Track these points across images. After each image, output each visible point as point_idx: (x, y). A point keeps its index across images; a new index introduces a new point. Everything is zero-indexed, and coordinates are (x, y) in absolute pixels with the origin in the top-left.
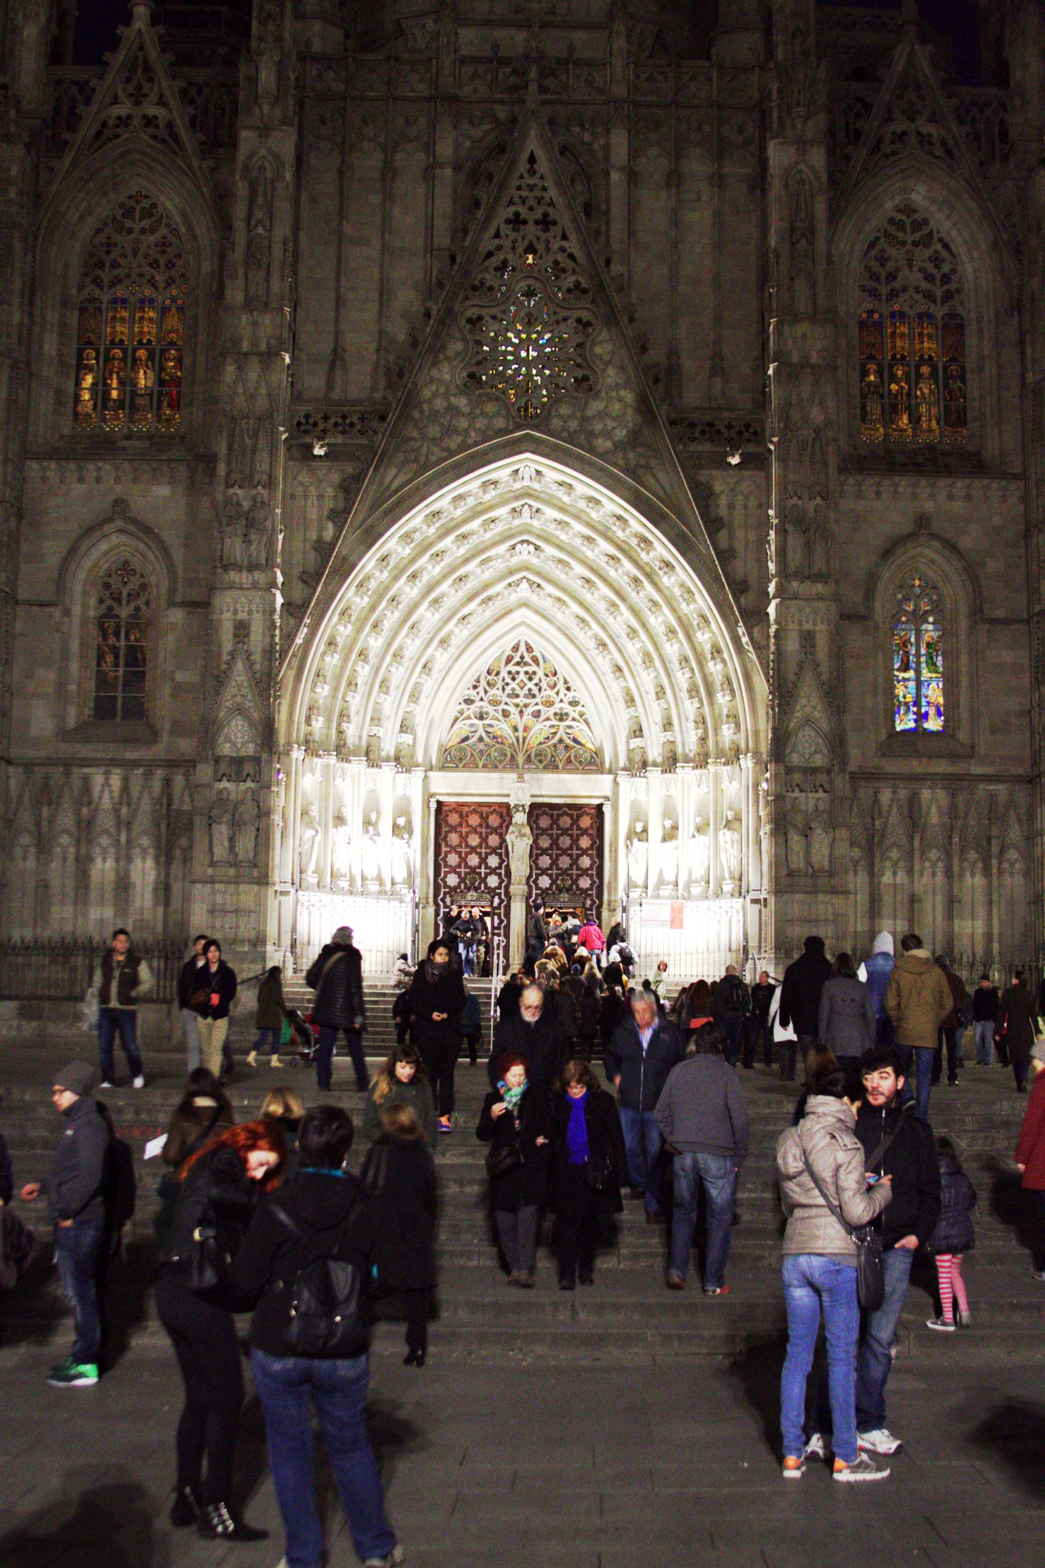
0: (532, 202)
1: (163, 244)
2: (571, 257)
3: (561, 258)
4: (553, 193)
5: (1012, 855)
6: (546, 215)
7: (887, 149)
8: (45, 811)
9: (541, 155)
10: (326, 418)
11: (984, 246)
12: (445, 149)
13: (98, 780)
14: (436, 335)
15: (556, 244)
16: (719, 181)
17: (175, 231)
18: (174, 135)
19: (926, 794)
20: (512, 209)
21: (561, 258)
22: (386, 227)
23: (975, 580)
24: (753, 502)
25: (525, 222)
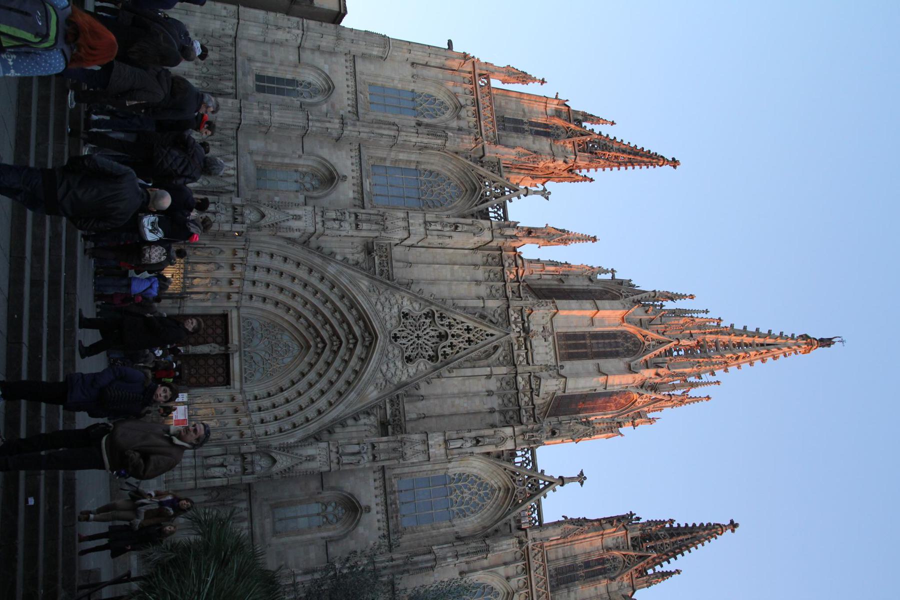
2: (458, 352)
4: (481, 343)
8: (218, 143)
12: (492, 304)
13: (232, 165)
14: (421, 298)
15: (461, 345)
16: (492, 411)
19: (245, 524)
24: (367, 433)
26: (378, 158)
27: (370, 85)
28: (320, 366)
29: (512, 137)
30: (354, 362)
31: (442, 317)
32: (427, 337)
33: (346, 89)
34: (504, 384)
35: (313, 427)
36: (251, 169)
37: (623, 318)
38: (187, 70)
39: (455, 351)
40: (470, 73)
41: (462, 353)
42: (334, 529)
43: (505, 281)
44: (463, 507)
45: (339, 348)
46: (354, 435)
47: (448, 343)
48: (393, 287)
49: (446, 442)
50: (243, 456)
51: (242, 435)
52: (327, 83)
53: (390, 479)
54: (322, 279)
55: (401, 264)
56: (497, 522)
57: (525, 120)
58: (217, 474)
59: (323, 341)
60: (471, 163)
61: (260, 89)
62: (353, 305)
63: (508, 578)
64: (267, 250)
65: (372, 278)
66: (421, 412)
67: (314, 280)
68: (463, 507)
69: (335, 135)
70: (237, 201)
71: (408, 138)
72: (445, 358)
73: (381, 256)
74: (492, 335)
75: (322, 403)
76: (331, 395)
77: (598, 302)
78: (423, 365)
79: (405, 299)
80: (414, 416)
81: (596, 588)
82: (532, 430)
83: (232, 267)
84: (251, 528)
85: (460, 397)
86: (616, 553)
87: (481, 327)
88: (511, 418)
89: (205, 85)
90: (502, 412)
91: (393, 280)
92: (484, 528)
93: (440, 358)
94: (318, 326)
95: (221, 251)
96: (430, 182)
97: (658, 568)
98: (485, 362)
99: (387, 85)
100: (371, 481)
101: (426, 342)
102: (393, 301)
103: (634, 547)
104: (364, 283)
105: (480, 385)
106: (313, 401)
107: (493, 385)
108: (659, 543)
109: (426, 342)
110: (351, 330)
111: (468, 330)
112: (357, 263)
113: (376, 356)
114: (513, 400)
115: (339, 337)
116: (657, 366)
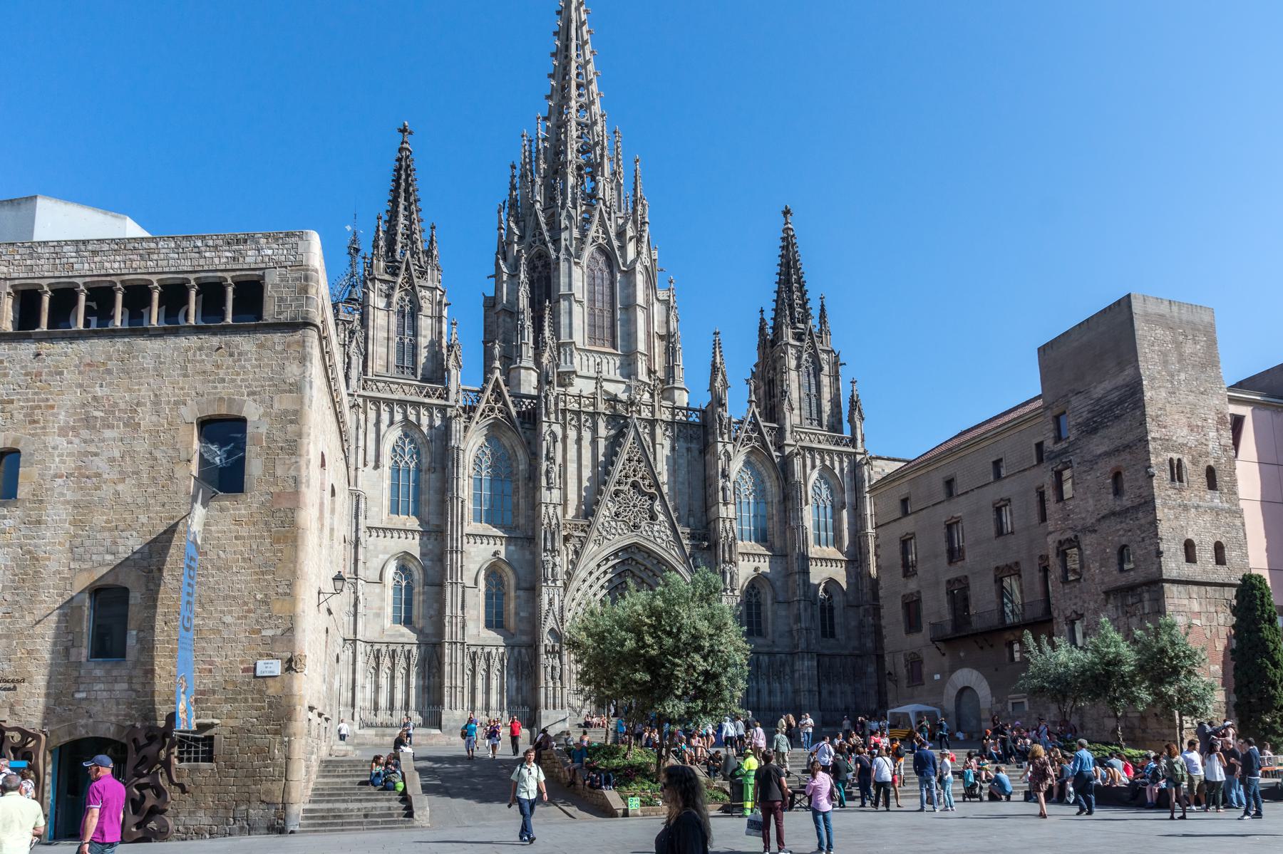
12: (602, 431)
31: (619, 483)
37: (576, 264)
40: (365, 401)
49: (726, 504)
60: (474, 424)
77: (563, 290)
78: (658, 507)
82: (721, 425)
86: (803, 361)
93: (653, 490)
97: (815, 312)
104: (591, 548)
107: (667, 443)
111: (630, 460)
112: (576, 552)
116: (621, 234)
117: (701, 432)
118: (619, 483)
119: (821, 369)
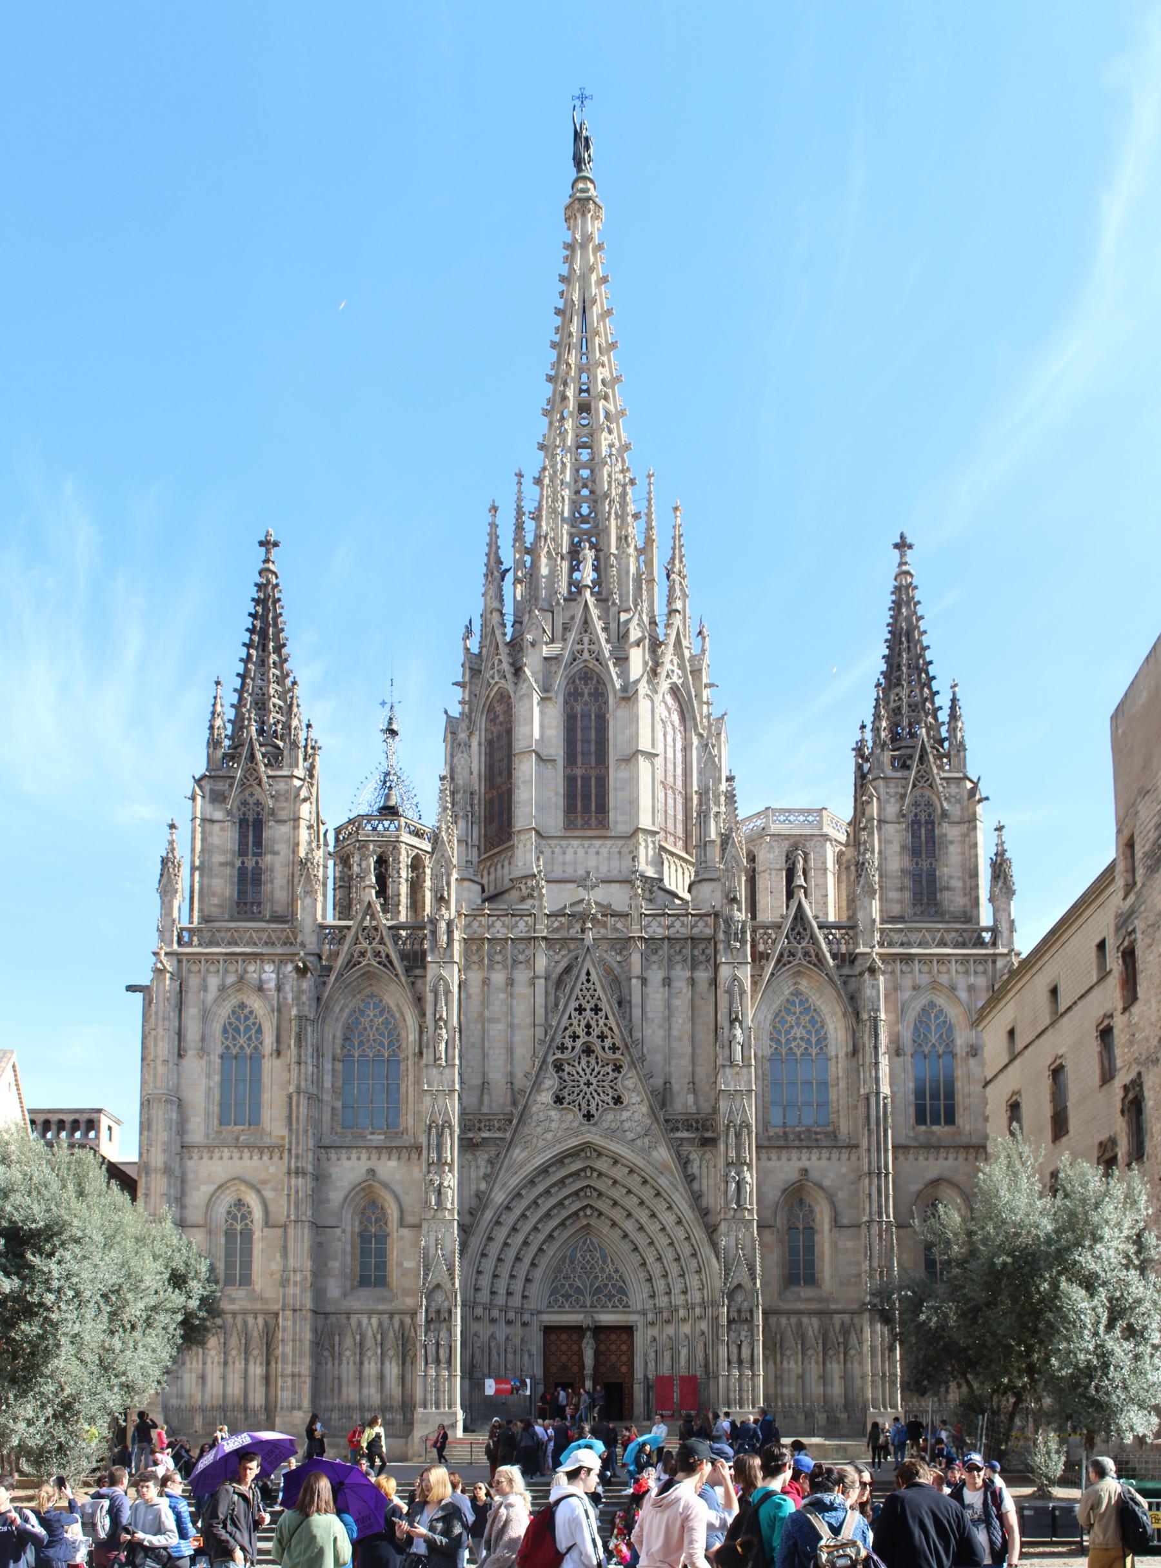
0: (588, 997)
1: (386, 1023)
2: (611, 1029)
3: (606, 1030)
4: (600, 992)
5: (852, 1352)
6: (596, 1005)
7: (785, 959)
8: (337, 1337)
9: (592, 971)
10: (480, 1121)
11: (840, 1014)
13: (365, 1320)
14: (537, 1076)
15: (601, 1023)
16: (692, 982)
17: (393, 1016)
18: (391, 962)
20: (578, 1002)
21: (606, 1030)
22: (511, 1011)
23: (833, 1205)
25: (585, 1010)
26: (332, 1119)
27: (221, 1124)
28: (617, 1215)
29: (272, 892)
30: (619, 1173)
32: (588, 1071)
33: (236, 1160)
34: (655, 958)
35: (699, 1234)
36: (364, 1292)
38: (236, 1376)
39: (609, 1033)
41: (612, 1022)
42: (821, 1213)
43: (507, 939)
44: (814, 1040)
45: (595, 1189)
46: (712, 1182)
47: (598, 1042)
48: (522, 1115)
50: (730, 1322)
51: (700, 1318)
52: (228, 1188)
53: (769, 1138)
54: (508, 1208)
55: (486, 1097)
56: (840, 995)
57: (238, 864)
58: (749, 1352)
59: (583, 1208)
61: (246, 1280)
62: (544, 1170)
63: (915, 988)
64: (474, 1276)
65: (511, 1143)
66: (686, 1086)
67: (510, 1219)
68: (814, 1040)
69: (313, 1184)
70: (421, 1318)
71: (310, 1079)
72: (618, 1049)
73: (480, 1129)
74: (588, 974)
75: (668, 1219)
76: (660, 1206)
79: (539, 1098)
80: (691, 1098)
81: (952, 842)
83: (493, 1321)
84: (811, 1313)
85: (670, 1029)
87: (577, 991)
88: (703, 952)
89: (255, 1352)
90: (693, 968)
91: (512, 1113)
92: (845, 1015)
94: (565, 1214)
95: (475, 1334)
96: (361, 1043)
98: (624, 984)
99: (217, 1097)
100: (770, 1164)
101: (595, 1073)
102: (542, 1116)
103: (905, 767)
104: (518, 1154)
105: (656, 995)
106: (663, 1229)
107: (656, 976)
108: (904, 710)
109: (595, 1073)
110: (576, 1174)
111: (580, 1010)
112: (490, 1162)
113: (615, 1147)
114: (678, 949)
115: (582, 1189)
117: (710, 951)
118: (562, 1048)
119: (945, 814)
